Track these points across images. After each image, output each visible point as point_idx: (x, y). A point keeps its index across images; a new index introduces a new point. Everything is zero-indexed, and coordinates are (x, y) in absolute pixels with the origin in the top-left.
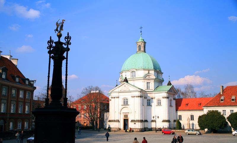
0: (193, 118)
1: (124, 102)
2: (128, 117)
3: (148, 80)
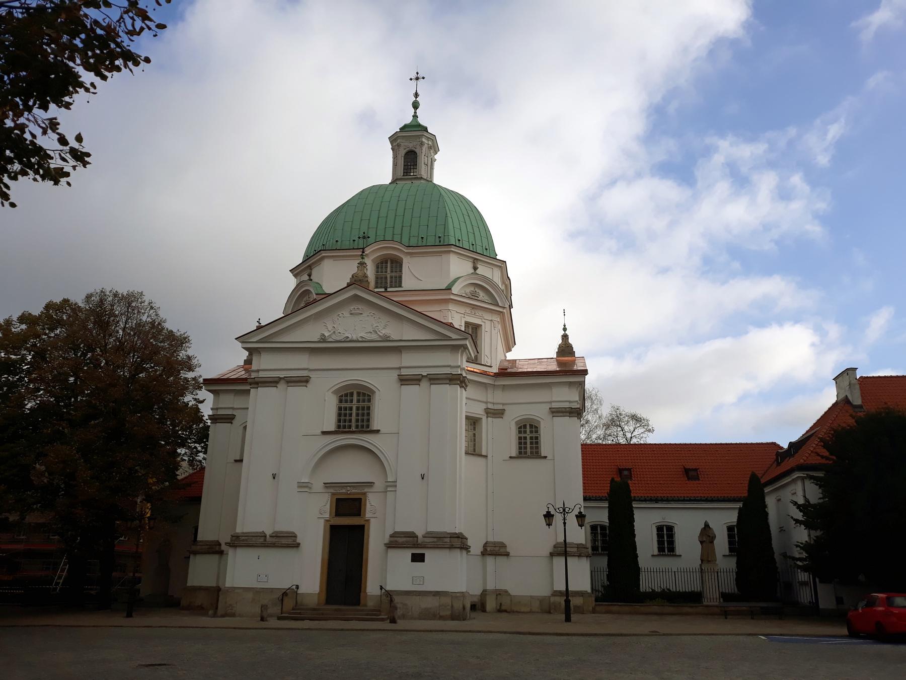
0: (671, 542)
1: (343, 416)
2: (368, 515)
3: (468, 310)
